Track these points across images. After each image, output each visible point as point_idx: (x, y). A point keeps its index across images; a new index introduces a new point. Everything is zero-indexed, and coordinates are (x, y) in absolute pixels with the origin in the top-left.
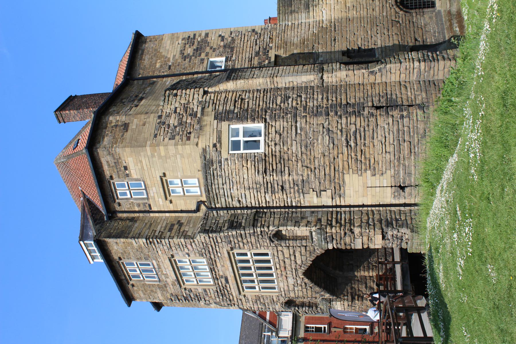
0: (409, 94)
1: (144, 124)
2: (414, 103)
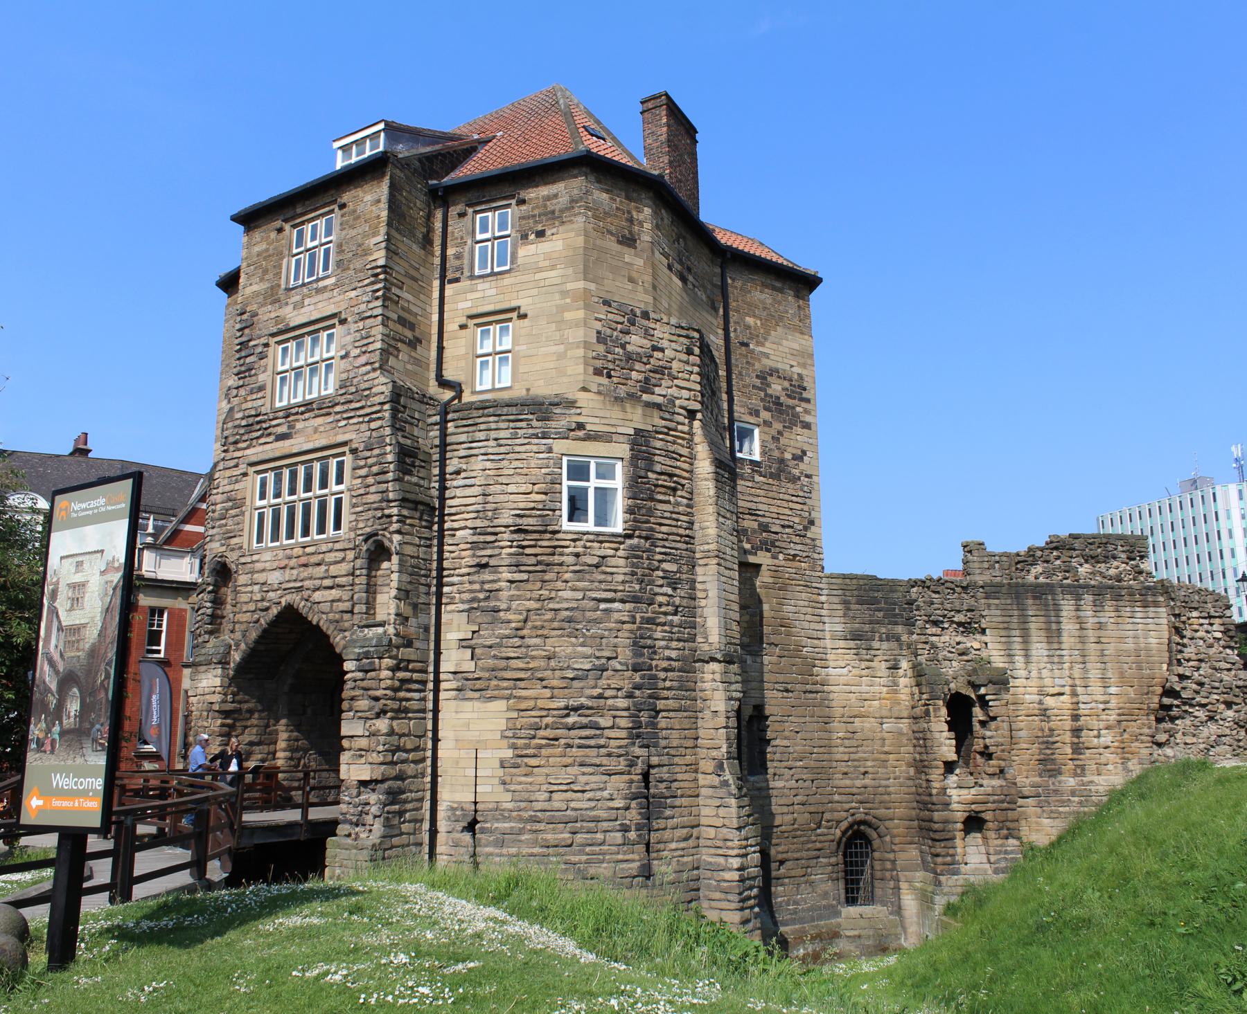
0: (673, 845)
1: (631, 280)
2: (654, 855)
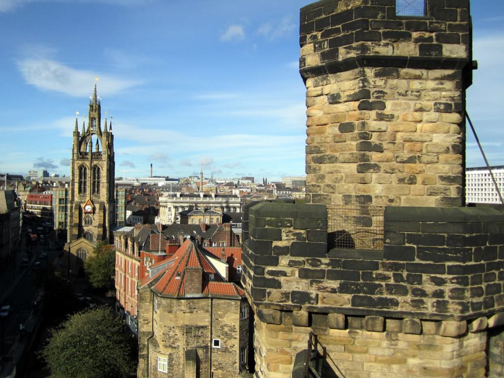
1: (171, 320)
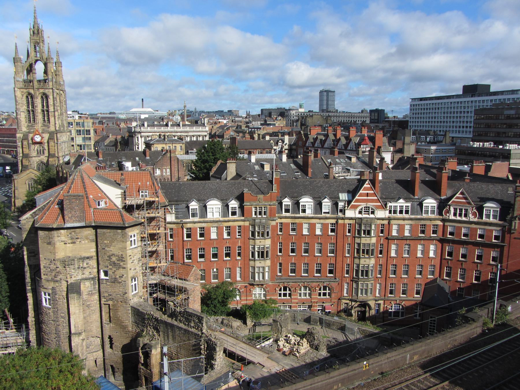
1: (50, 253)
